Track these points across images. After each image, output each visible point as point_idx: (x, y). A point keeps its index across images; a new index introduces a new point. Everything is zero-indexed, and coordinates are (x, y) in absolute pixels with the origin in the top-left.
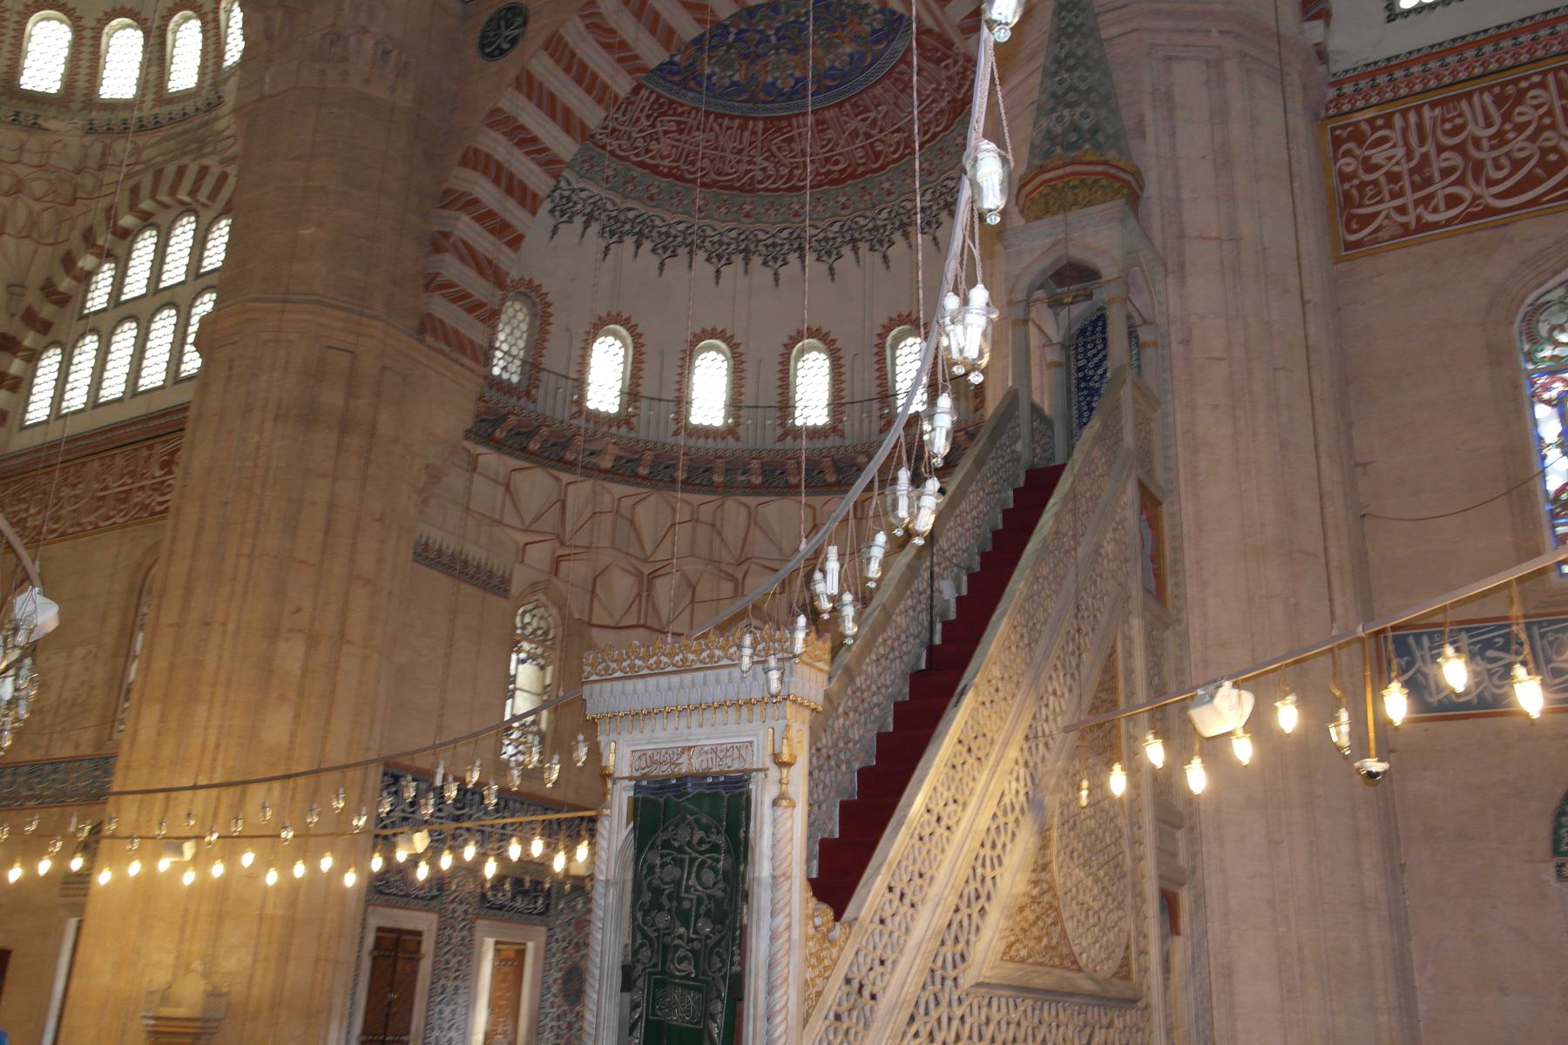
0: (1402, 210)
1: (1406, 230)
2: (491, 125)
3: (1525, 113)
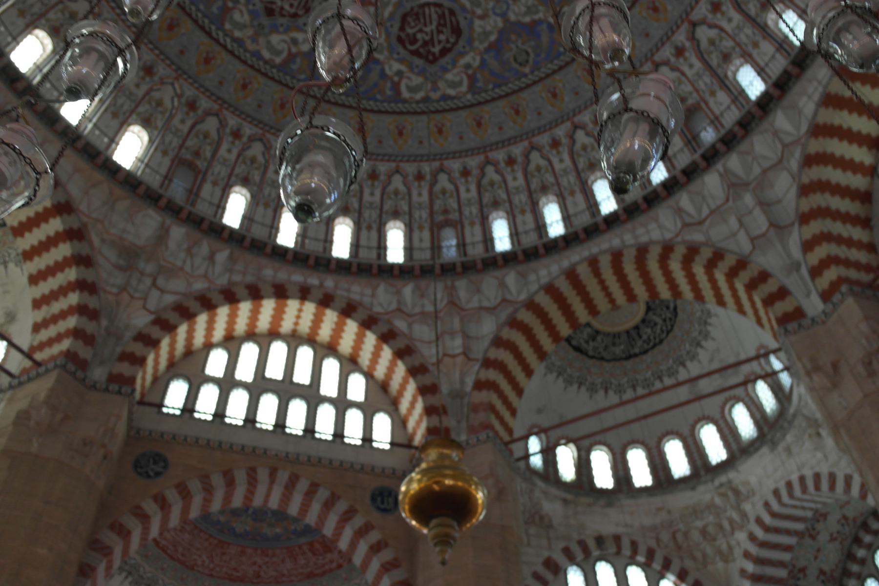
2: (135, 515)
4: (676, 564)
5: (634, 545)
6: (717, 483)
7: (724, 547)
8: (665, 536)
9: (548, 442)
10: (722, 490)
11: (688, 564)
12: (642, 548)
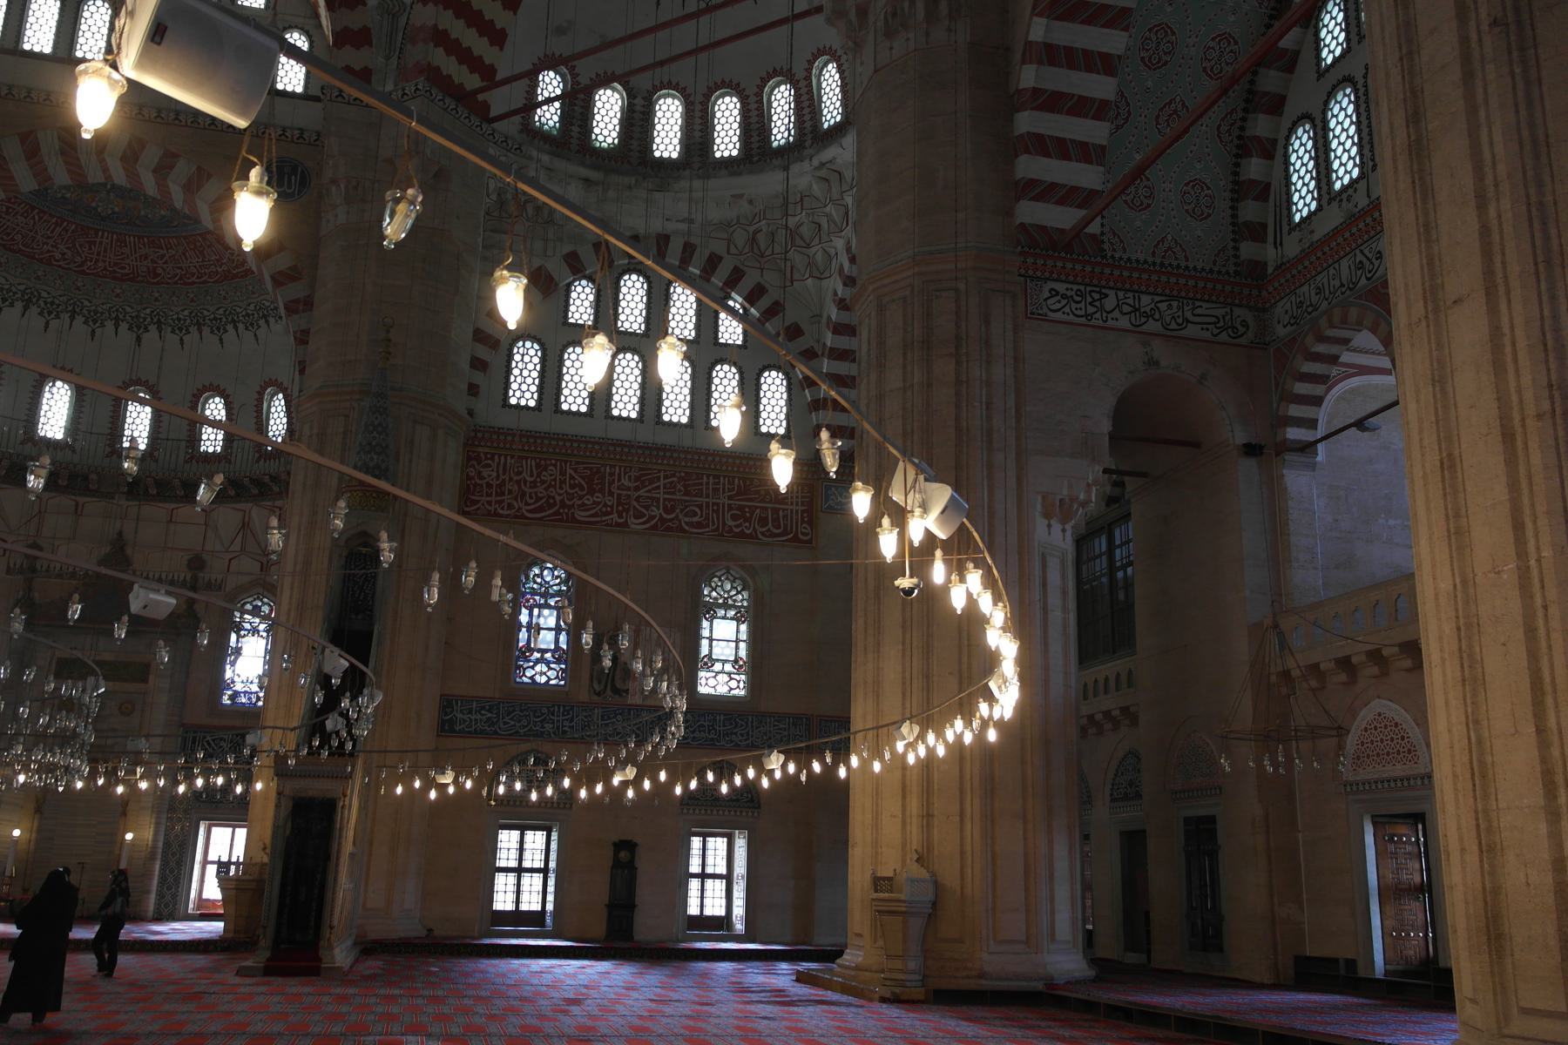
0: (489, 503)
1: (489, 514)
3: (546, 476)
4: (748, 282)
5: (688, 250)
6: (815, 162)
7: (819, 257)
8: (740, 238)
9: (575, 83)
10: (823, 173)
11: (771, 279)
12: (700, 257)
